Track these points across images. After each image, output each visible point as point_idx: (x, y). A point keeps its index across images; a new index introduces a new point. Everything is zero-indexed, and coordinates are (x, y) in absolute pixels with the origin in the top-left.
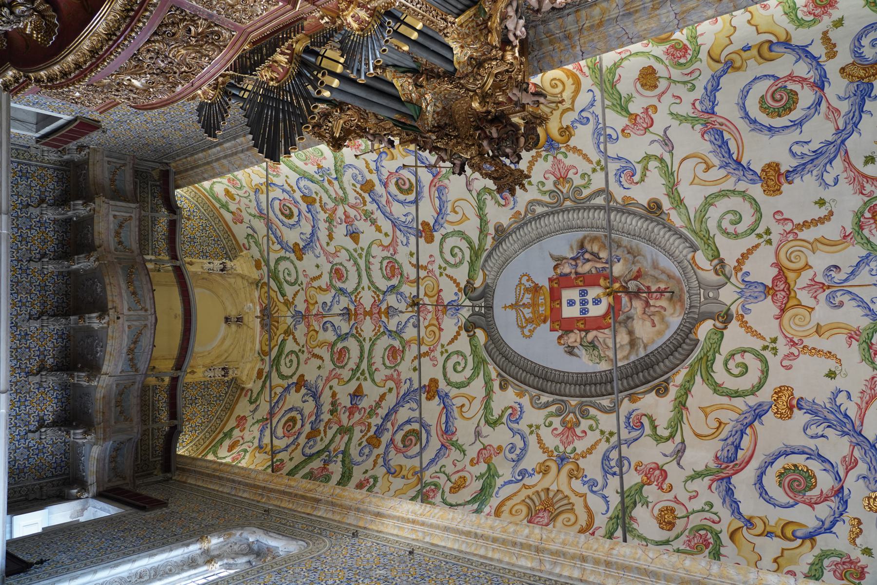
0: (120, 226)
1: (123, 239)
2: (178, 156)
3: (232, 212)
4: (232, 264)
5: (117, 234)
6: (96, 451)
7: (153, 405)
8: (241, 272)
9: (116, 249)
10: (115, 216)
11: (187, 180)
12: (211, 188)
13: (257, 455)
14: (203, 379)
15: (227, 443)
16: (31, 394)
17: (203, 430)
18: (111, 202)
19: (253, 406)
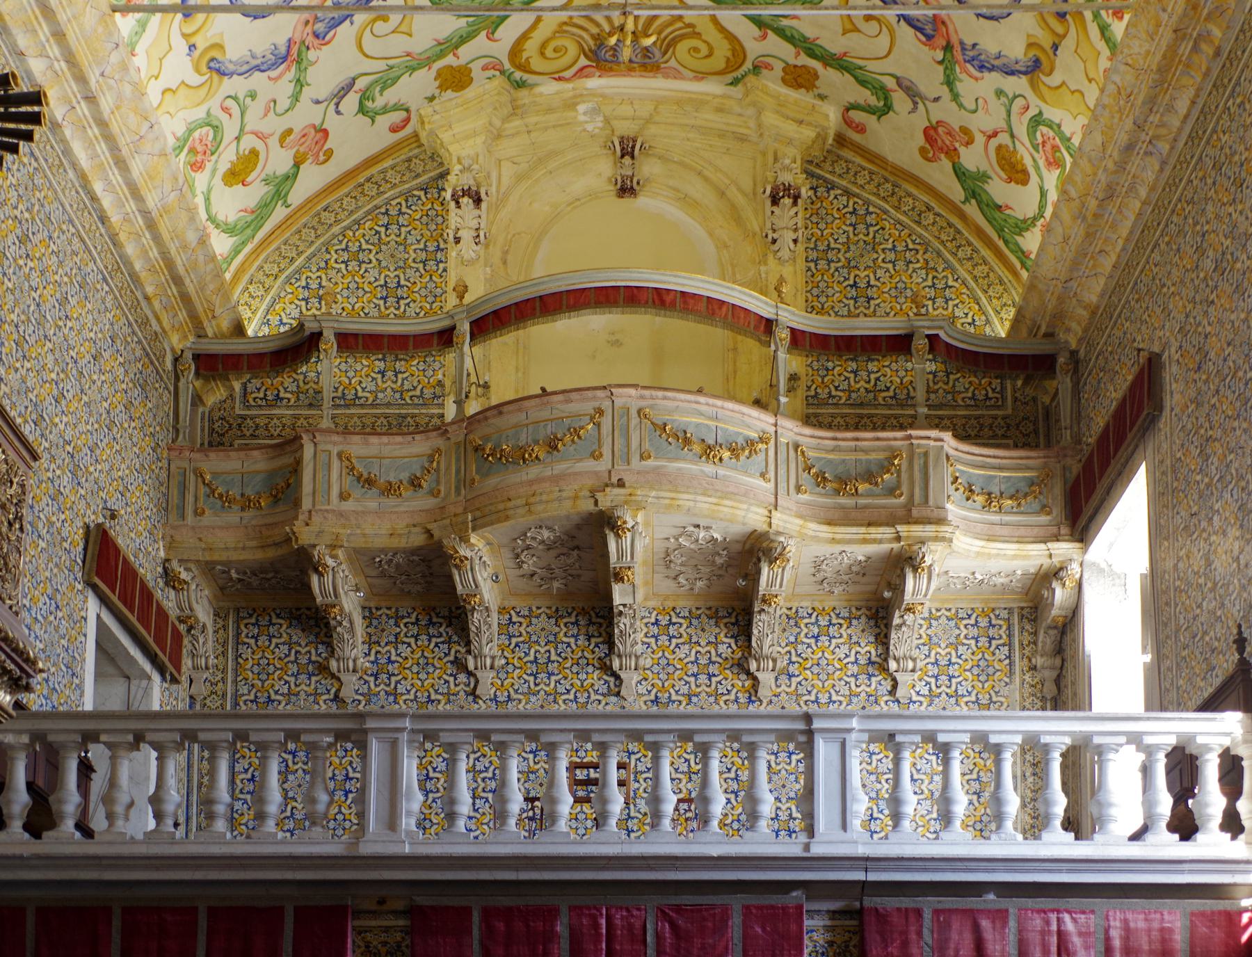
0: (370, 482)
1: (405, 476)
2: (145, 323)
3: (297, 165)
4: (456, 168)
5: (390, 490)
6: (964, 542)
7: (861, 405)
8: (480, 140)
9: (434, 493)
10: (343, 497)
11: (217, 301)
12: (230, 230)
13: (1055, 79)
14: (802, 263)
15: (999, 189)
16: (801, 690)
18: (306, 504)
19: (900, 101)
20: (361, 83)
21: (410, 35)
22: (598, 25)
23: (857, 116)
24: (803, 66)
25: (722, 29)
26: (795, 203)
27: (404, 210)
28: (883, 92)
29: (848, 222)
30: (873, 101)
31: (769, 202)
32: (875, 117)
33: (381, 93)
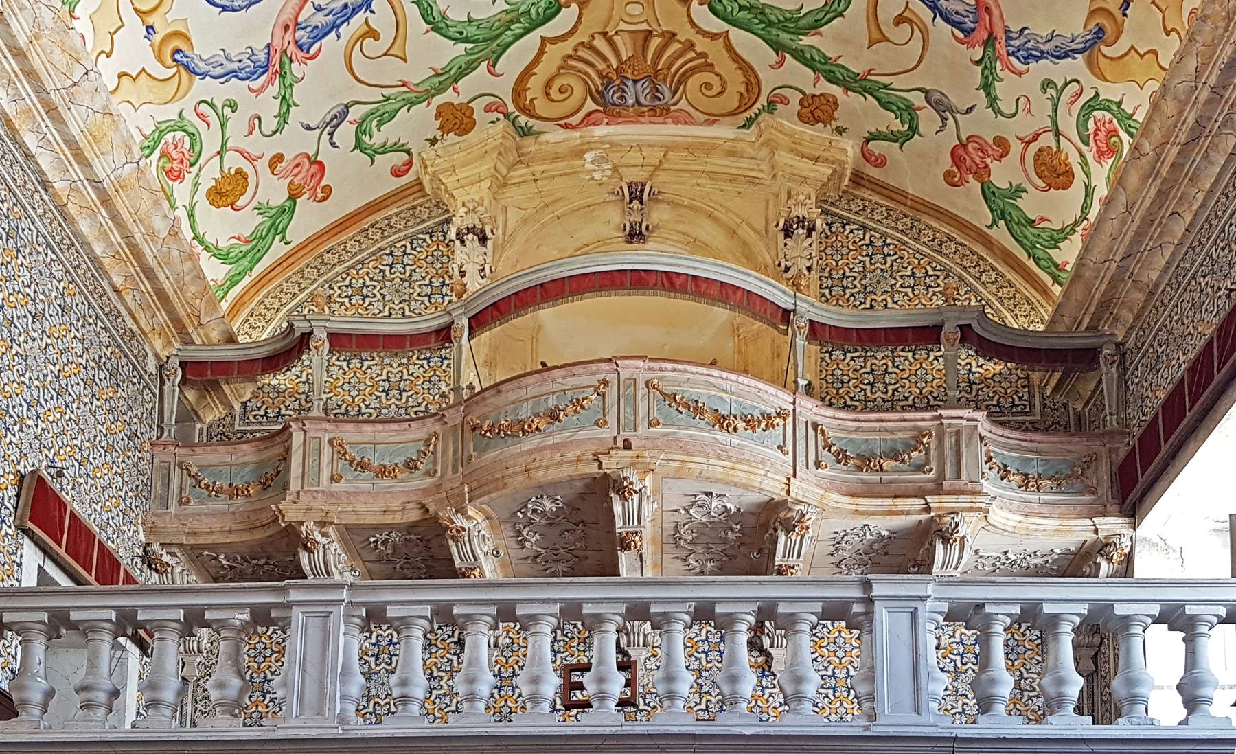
17: (972, 289)
20: (356, 113)
21: (405, 61)
22: (605, 59)
23: (876, 147)
24: (822, 95)
25: (736, 58)
26: (809, 235)
27: (408, 251)
28: (909, 113)
29: (864, 253)
30: (897, 126)
31: (782, 235)
32: (897, 145)
33: (379, 126)
